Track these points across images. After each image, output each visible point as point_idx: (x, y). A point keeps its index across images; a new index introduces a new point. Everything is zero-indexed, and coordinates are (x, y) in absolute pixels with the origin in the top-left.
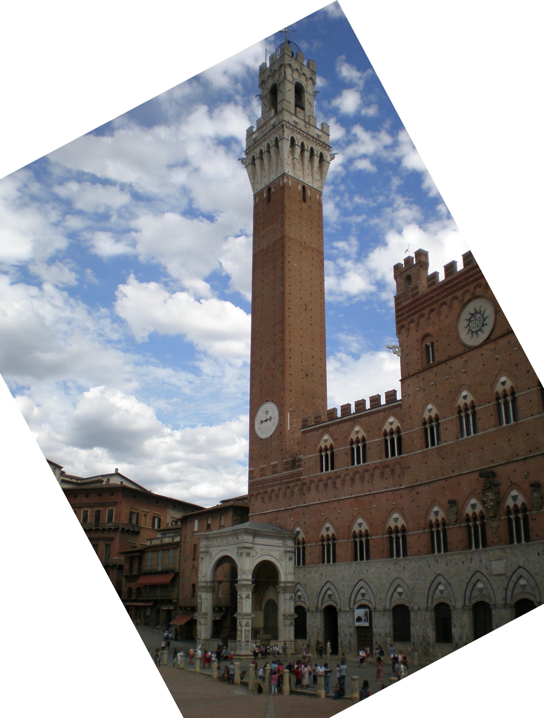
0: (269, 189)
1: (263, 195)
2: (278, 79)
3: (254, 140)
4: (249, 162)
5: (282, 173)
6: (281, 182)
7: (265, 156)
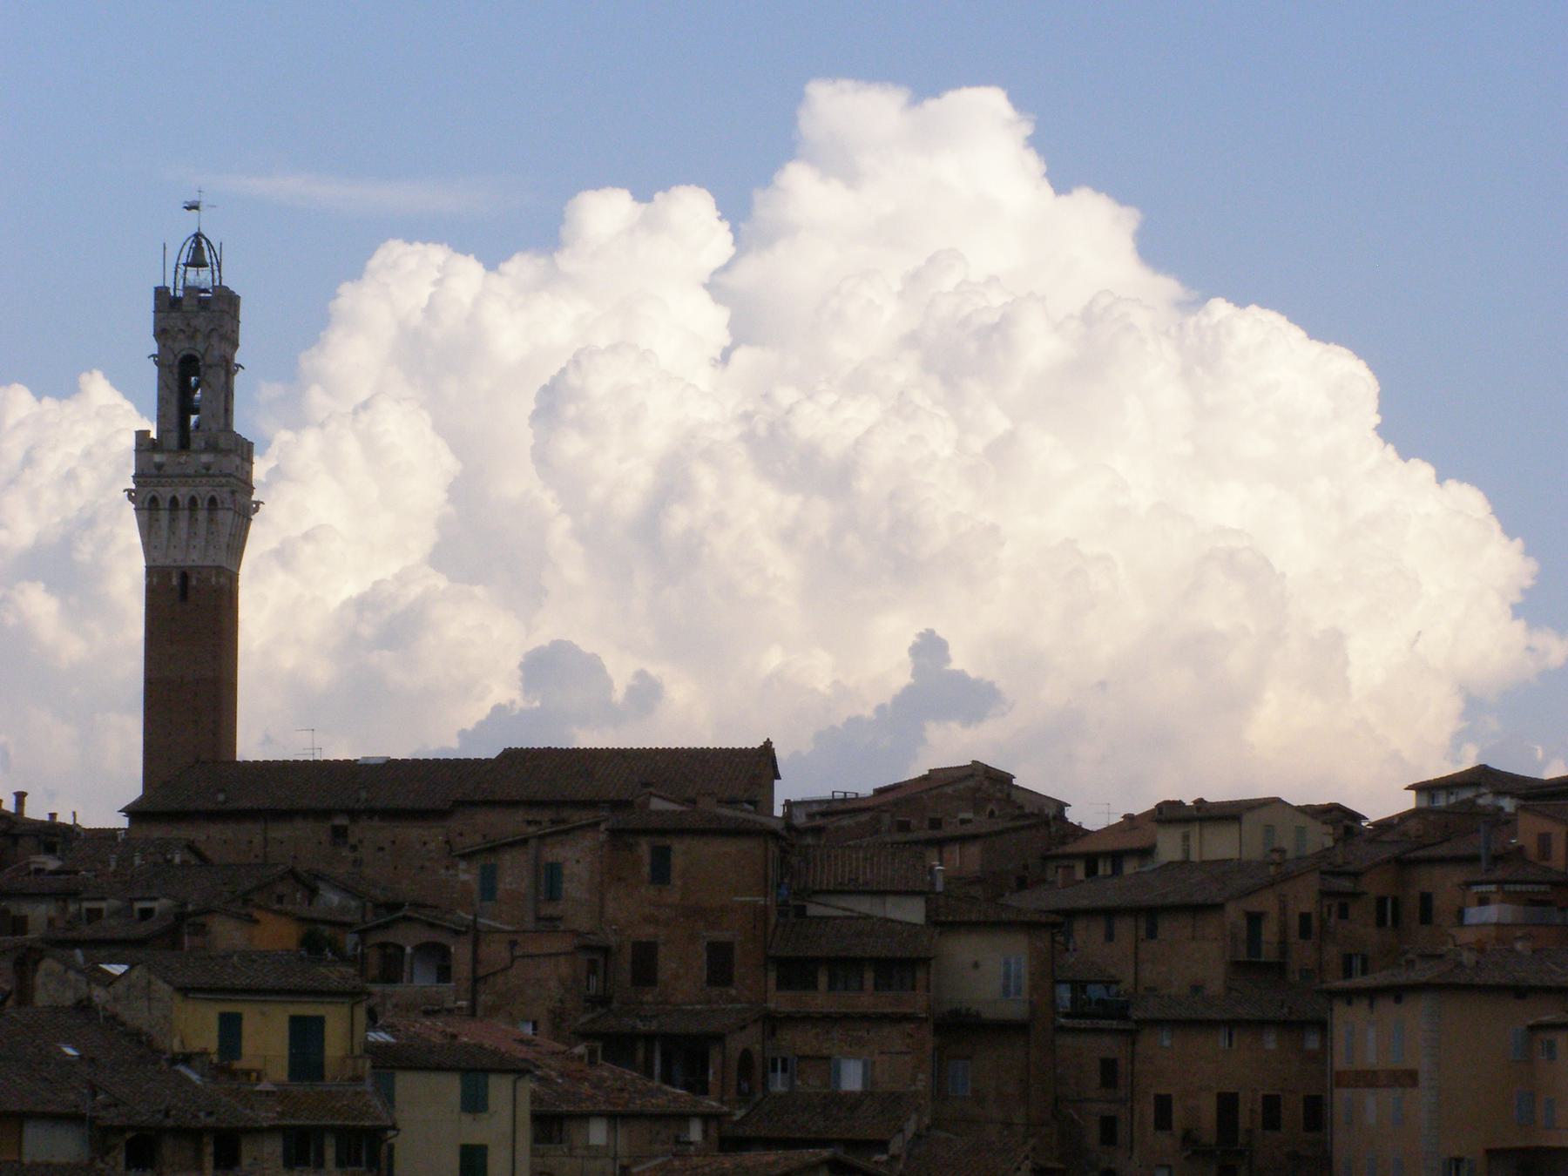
0: (184, 577)
1: (170, 580)
2: (202, 351)
3: (159, 466)
4: (143, 503)
5: (216, 564)
6: (213, 579)
7: (184, 515)
